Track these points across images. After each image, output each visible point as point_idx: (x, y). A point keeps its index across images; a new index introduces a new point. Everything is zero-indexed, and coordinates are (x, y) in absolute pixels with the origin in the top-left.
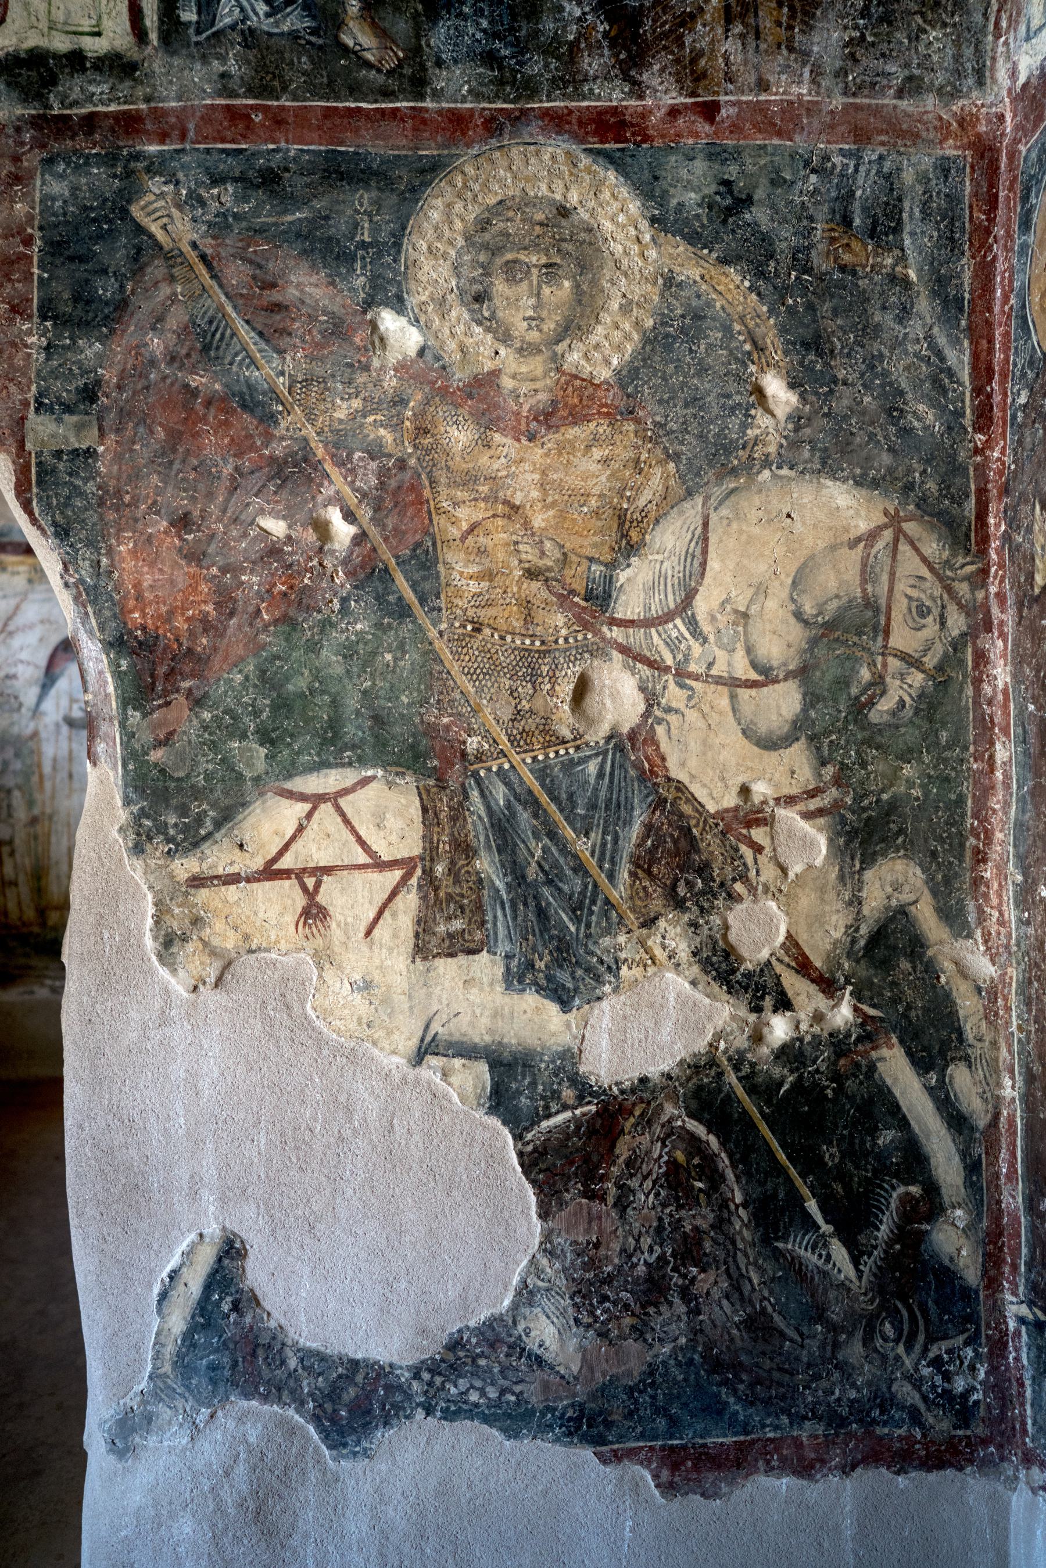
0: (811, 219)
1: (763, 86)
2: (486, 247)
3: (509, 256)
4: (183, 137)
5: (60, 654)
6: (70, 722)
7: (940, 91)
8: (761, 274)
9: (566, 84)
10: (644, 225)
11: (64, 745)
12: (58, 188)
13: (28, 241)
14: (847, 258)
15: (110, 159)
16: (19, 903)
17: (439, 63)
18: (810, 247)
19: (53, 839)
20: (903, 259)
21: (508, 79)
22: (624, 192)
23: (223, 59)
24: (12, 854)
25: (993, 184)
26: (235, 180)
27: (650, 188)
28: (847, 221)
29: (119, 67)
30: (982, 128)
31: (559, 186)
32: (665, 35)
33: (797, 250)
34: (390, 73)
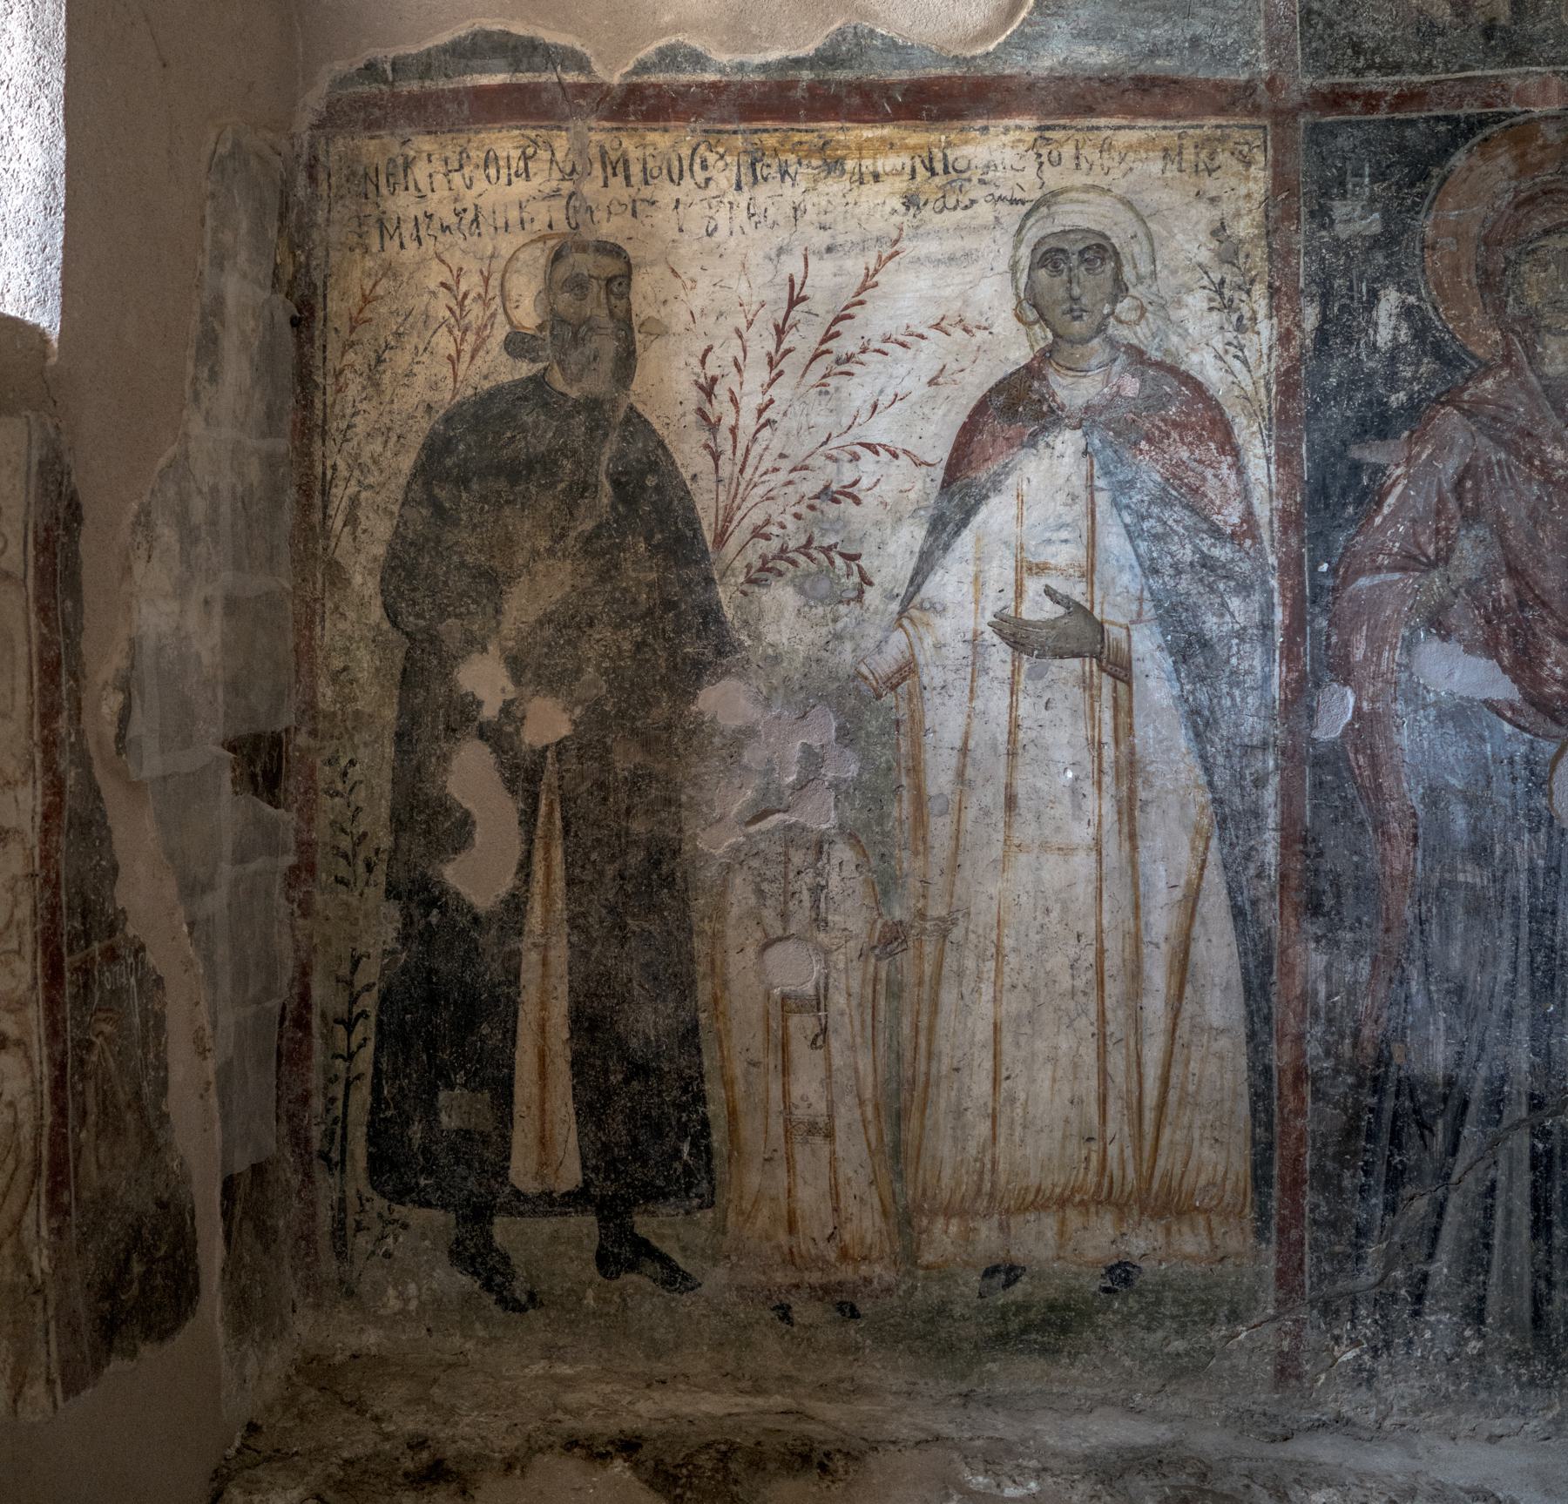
5: (994, 424)
6: (1017, 635)
11: (996, 702)
19: (948, 997)
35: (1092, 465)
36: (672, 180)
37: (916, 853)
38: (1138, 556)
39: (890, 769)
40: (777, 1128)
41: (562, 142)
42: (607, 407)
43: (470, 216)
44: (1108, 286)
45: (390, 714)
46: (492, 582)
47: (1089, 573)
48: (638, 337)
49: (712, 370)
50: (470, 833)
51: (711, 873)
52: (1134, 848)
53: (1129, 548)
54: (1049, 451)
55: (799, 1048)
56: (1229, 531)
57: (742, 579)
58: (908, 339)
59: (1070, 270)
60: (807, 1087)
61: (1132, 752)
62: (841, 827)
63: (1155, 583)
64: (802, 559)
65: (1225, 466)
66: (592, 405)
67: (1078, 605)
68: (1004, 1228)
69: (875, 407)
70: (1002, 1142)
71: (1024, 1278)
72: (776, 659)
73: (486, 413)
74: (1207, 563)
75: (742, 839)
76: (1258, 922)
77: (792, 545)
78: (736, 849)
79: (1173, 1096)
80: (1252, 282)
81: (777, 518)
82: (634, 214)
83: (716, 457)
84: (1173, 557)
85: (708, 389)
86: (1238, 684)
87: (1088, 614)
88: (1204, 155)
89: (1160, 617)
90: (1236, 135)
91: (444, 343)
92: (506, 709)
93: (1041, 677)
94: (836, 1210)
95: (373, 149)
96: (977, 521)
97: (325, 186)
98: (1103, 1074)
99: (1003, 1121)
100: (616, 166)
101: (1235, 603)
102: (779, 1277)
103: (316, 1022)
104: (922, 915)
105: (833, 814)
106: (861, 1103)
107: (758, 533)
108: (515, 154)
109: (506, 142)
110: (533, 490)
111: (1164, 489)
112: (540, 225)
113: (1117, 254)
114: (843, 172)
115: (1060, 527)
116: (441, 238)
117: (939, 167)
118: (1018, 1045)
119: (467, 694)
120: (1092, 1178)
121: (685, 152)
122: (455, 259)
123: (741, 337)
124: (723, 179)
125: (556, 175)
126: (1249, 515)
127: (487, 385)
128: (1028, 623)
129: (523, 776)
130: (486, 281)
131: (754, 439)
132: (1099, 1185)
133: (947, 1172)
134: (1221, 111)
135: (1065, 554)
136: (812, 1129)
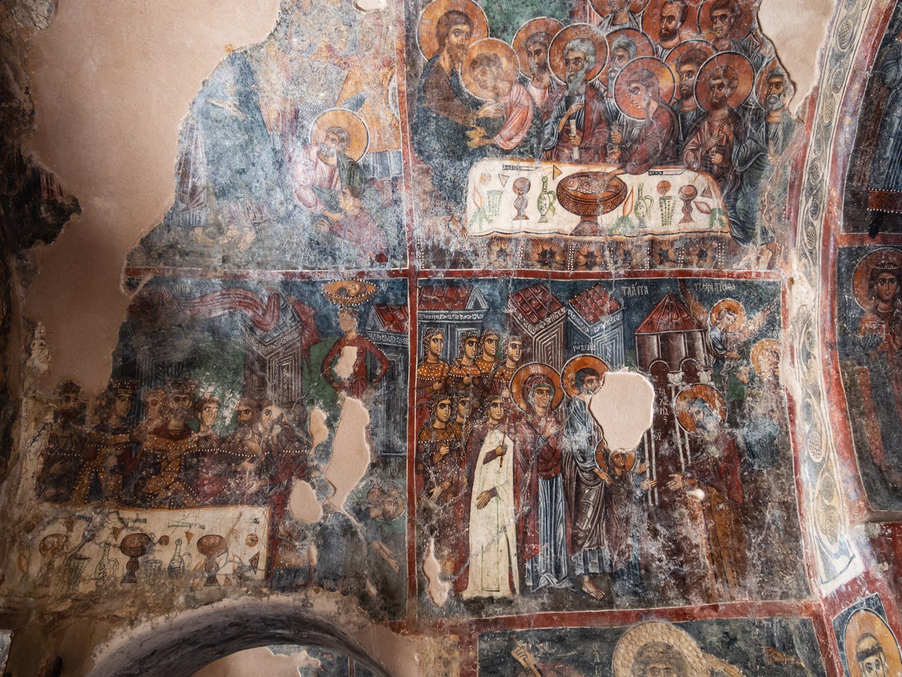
0: (760, 645)
1: (732, 598)
2: (642, 662)
3: (652, 666)
4: (529, 626)
7: (795, 596)
8: (746, 667)
9: (663, 601)
10: (699, 650)
12: (484, 645)
13: (475, 667)
14: (777, 659)
15: (503, 634)
17: (617, 596)
18: (762, 655)
20: (797, 658)
21: (642, 600)
22: (689, 638)
23: (542, 598)
25: (823, 628)
26: (548, 640)
27: (699, 636)
28: (773, 645)
29: (506, 602)
30: (814, 608)
31: (665, 638)
32: (695, 583)
33: (757, 657)
34: (601, 600)
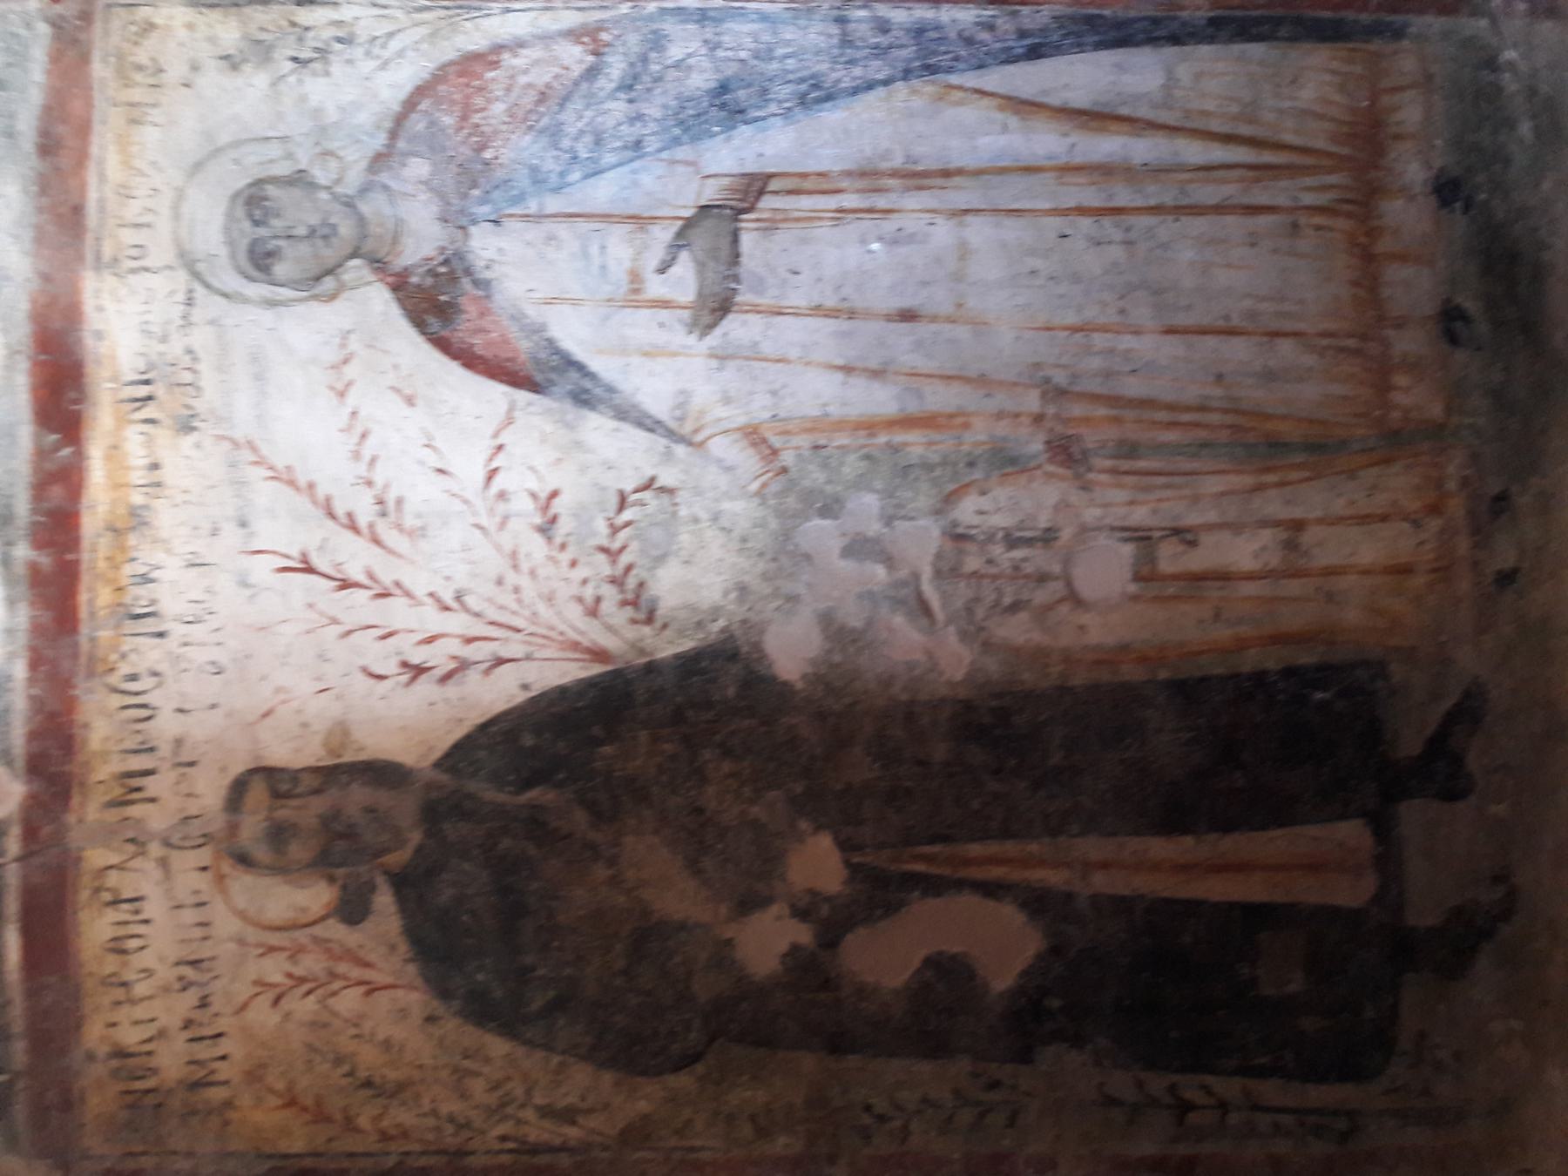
5: (462, 331)
6: (716, 307)
11: (792, 333)
16: (1364, 519)
19: (1133, 387)
24: (1185, 535)
35: (511, 216)
36: (149, 718)
37: (966, 426)
38: (620, 164)
39: (868, 457)
40: (1293, 587)
41: (96, 857)
42: (434, 795)
43: (188, 971)
44: (296, 193)
45: (808, 1062)
46: (650, 936)
47: (640, 221)
48: (347, 758)
49: (390, 667)
50: (953, 957)
51: (993, 666)
52: (960, 172)
53: (610, 175)
54: (496, 267)
55: (1196, 561)
56: (591, 58)
57: (647, 630)
58: (359, 430)
59: (276, 237)
60: (1245, 552)
61: (848, 174)
62: (938, 512)
63: (652, 144)
64: (625, 559)
65: (516, 62)
66: (434, 812)
67: (680, 234)
68: (1400, 323)
69: (441, 471)
70: (1301, 326)
71: (1459, 300)
72: (743, 589)
73: (438, 948)
74: (627, 86)
75: (952, 629)
76: (1044, 30)
77: (607, 570)
78: (964, 636)
79: (1245, 130)
80: (293, 24)
81: (575, 590)
82: (191, 764)
83: (500, 662)
84: (620, 125)
85: (418, 671)
86: (771, 50)
87: (689, 224)
88: (138, 77)
89: (695, 139)
90: (115, 39)
91: (349, 1001)
92: (802, 913)
93: (761, 280)
94: (1384, 518)
95: (99, 1099)
96: (579, 354)
97: (143, 1159)
98: (1220, 209)
99: (1275, 325)
100: (131, 787)
101: (675, 52)
102: (1464, 585)
103: (1182, 1149)
104: (1038, 419)
105: (922, 522)
106: (1260, 488)
107: (593, 612)
108: (112, 915)
109: (95, 928)
110: (535, 885)
111: (541, 132)
112: (202, 882)
113: (260, 182)
114: (146, 507)
115: (585, 255)
116: (214, 1009)
117: (143, 391)
118: (1189, 307)
119: (783, 963)
120: (1342, 223)
121: (116, 701)
122: (243, 991)
123: (349, 632)
124: (149, 654)
125: (137, 863)
126: (574, 35)
127: (403, 947)
128: (700, 295)
129: (878, 893)
130: (272, 949)
131: (477, 615)
132: (1349, 215)
133: (1338, 389)
134: (85, 59)
135: (619, 249)
136: (1291, 546)
